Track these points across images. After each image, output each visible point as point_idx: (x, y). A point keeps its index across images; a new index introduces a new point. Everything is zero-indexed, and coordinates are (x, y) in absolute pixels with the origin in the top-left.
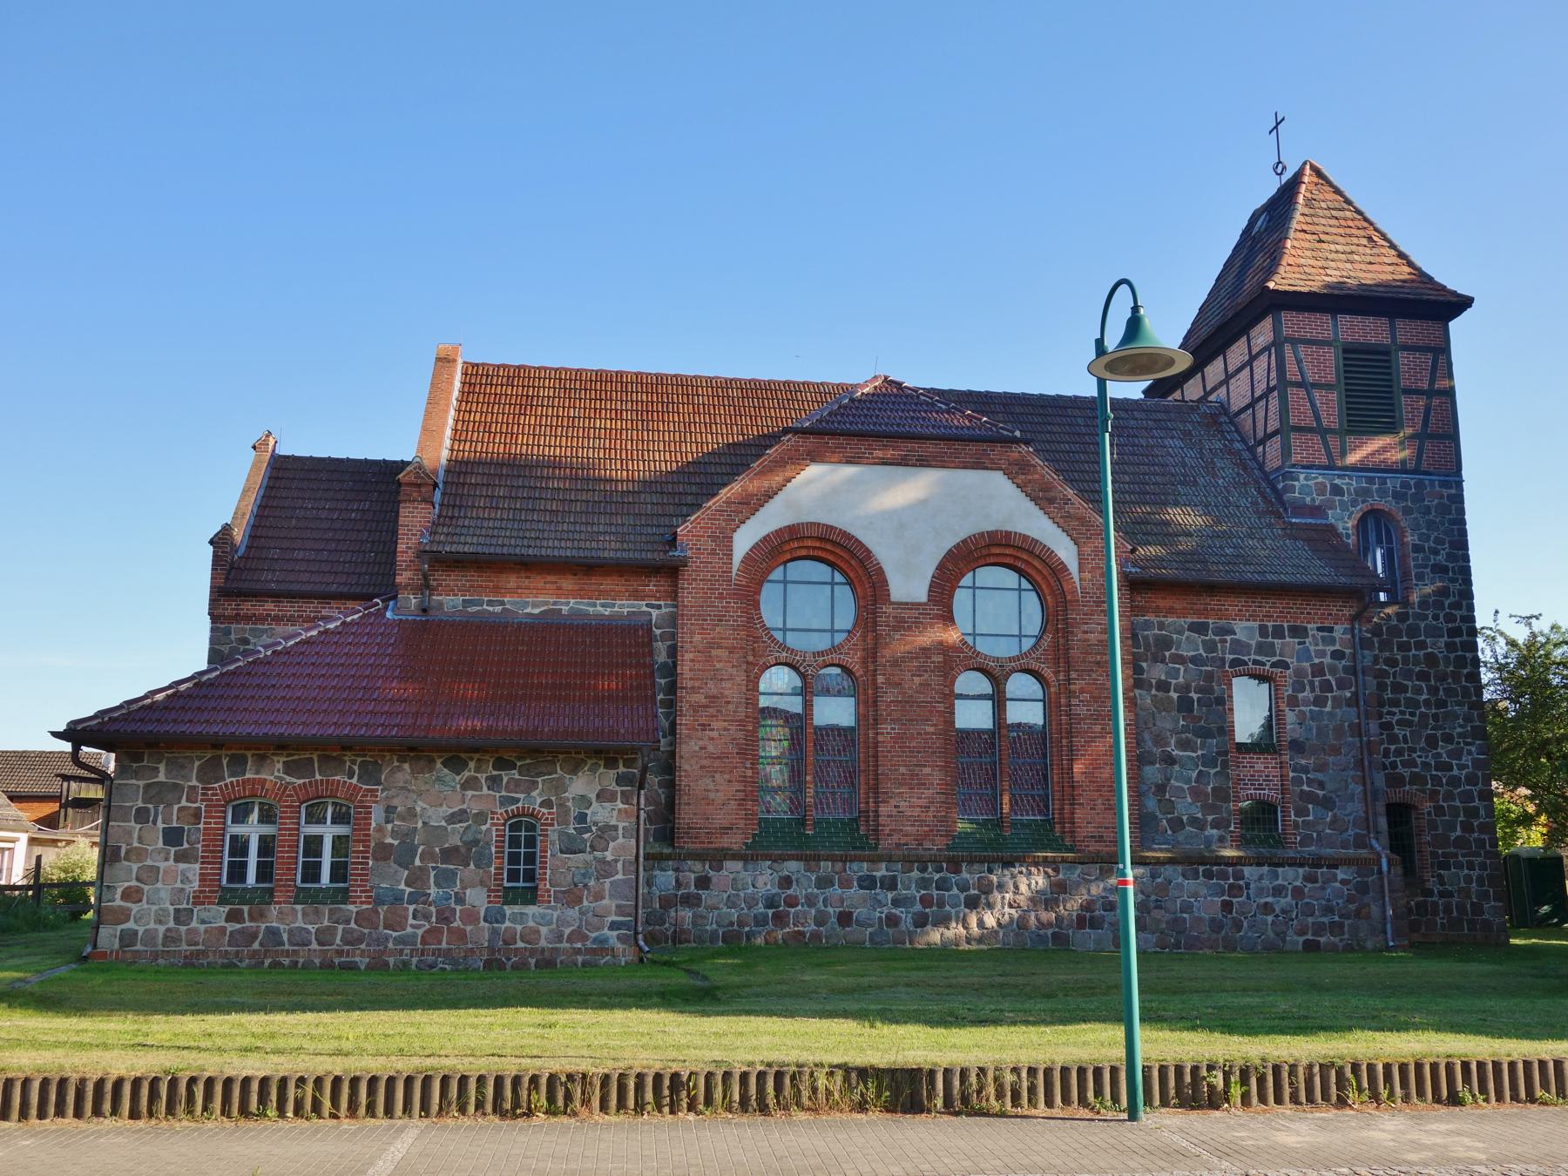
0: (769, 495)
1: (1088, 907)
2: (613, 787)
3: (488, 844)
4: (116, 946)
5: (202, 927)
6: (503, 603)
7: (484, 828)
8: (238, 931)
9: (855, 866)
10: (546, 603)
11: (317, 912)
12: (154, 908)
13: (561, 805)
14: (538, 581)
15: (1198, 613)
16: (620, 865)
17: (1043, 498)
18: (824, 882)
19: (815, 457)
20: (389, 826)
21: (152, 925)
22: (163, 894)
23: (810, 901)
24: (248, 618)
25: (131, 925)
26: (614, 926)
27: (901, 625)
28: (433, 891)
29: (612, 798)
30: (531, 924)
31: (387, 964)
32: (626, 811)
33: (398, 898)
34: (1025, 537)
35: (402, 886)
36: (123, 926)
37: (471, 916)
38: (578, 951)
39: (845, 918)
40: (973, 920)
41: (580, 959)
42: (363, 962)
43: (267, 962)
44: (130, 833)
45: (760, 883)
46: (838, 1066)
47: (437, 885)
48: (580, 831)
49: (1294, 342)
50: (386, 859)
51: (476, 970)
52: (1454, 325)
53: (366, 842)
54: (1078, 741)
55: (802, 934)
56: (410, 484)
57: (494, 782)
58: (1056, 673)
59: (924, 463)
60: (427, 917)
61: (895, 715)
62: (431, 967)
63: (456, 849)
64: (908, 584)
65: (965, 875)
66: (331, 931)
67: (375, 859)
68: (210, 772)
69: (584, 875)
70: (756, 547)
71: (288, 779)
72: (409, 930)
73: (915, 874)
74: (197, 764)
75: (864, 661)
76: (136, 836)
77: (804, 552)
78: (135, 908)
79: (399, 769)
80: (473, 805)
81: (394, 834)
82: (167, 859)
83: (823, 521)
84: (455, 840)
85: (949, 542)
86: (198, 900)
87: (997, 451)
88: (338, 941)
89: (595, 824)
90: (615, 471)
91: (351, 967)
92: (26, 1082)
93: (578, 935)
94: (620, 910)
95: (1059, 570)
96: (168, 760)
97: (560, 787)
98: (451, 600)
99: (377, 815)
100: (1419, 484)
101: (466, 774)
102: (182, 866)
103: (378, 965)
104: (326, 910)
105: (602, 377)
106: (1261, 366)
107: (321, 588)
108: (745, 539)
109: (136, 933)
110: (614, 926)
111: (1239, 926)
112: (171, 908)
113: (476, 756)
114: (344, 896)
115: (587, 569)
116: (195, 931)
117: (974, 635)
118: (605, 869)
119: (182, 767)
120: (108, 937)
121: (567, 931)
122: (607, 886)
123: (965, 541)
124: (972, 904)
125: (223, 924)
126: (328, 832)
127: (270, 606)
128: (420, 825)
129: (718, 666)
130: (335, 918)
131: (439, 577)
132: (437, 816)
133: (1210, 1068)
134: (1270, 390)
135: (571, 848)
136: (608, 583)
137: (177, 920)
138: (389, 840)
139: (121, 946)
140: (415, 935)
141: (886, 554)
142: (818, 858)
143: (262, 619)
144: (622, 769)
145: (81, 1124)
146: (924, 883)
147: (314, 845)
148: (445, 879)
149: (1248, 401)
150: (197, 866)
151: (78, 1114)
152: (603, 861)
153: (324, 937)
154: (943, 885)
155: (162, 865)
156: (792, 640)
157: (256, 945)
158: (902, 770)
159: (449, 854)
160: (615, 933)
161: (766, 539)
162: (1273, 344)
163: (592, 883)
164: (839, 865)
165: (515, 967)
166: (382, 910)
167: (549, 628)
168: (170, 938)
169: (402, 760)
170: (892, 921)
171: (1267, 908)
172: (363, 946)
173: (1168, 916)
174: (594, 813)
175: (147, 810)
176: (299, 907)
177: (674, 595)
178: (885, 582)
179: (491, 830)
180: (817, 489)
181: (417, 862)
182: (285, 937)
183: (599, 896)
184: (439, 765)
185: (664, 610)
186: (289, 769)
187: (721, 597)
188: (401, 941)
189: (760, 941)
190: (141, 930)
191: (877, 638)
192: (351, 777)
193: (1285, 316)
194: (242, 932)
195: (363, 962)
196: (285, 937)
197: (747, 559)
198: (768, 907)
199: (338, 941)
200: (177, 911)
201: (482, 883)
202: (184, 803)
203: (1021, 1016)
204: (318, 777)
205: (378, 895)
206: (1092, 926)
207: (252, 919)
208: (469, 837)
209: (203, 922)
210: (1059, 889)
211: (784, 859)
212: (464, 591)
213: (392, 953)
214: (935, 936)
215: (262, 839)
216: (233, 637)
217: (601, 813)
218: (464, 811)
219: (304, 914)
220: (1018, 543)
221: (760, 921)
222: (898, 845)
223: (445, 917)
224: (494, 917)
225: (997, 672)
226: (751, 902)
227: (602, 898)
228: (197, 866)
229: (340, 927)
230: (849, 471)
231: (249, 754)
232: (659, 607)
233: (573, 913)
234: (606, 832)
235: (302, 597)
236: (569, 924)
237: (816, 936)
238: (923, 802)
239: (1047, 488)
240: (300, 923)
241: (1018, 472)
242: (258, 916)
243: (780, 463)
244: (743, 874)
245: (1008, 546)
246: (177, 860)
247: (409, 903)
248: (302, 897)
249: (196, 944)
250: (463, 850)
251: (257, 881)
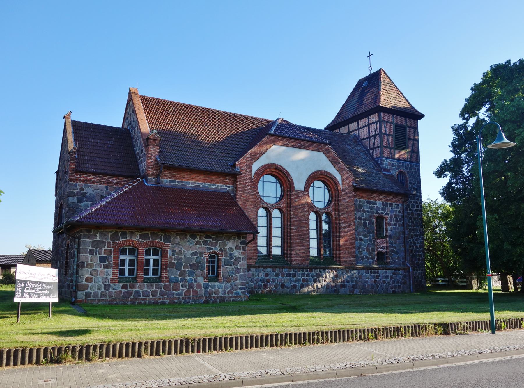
0: (262, 154)
1: (343, 282)
2: (240, 245)
3: (204, 263)
4: (84, 298)
5: (114, 291)
6: (182, 182)
7: (202, 257)
8: (126, 292)
9: (285, 270)
10: (195, 183)
11: (151, 285)
12: (97, 284)
13: (225, 251)
14: (193, 176)
15: (369, 198)
16: (242, 270)
17: (333, 162)
18: (277, 275)
19: (274, 142)
20: (173, 257)
21: (96, 291)
22: (100, 280)
23: (273, 281)
24: (83, 181)
25: (89, 290)
26: (240, 289)
27: (297, 197)
28: (187, 278)
29: (240, 249)
30: (217, 288)
31: (175, 302)
32: (243, 253)
33: (177, 280)
34: (329, 173)
35: (178, 277)
36: (86, 291)
37: (199, 286)
38: (231, 297)
39: (283, 286)
40: (315, 285)
41: (232, 299)
42: (167, 301)
43: (137, 302)
44: (88, 258)
45: (260, 275)
46: (440, 325)
47: (189, 276)
48: (231, 259)
49: (385, 122)
50: (173, 267)
51: (202, 303)
53: (166, 262)
54: (342, 234)
55: (271, 291)
56: (152, 139)
57: (205, 243)
58: (335, 214)
59: (304, 148)
60: (186, 287)
61: (296, 224)
62: (188, 303)
63: (194, 264)
64: (299, 185)
65: (313, 273)
66: (156, 291)
67: (169, 268)
68: (115, 237)
69: (232, 273)
70: (258, 170)
71: (141, 240)
72: (181, 291)
73: (301, 272)
74: (110, 234)
75: (287, 208)
76: (90, 259)
77: (270, 173)
78: (90, 284)
79: (176, 238)
80: (199, 250)
81: (175, 259)
82: (101, 267)
83: (277, 163)
84: (194, 262)
85: (310, 173)
86: (112, 281)
87: (322, 146)
88: (158, 295)
89: (235, 256)
90: (202, 139)
91: (164, 303)
92: (241, 337)
93: (230, 292)
94: (242, 284)
95: (336, 183)
96: (100, 232)
97: (224, 245)
98: (165, 181)
99: (170, 253)
100: (411, 165)
101: (197, 240)
102: (106, 270)
103: (172, 303)
104: (154, 284)
105: (190, 107)
106: (373, 127)
107: (109, 172)
108: (255, 167)
109: (91, 293)
110: (240, 289)
111: (378, 287)
112: (103, 284)
113: (200, 234)
114: (160, 279)
115: (208, 173)
116: (112, 292)
117: (313, 201)
118: (238, 271)
119: (105, 235)
120: (81, 295)
121: (227, 291)
122: (238, 276)
123: (314, 173)
124: (315, 281)
125: (121, 290)
126: (151, 258)
127: (92, 177)
128: (183, 256)
129: (248, 207)
130: (157, 287)
131: (165, 173)
132: (188, 253)
133: (498, 321)
134: (376, 134)
135: (228, 264)
136: (214, 178)
137: (105, 289)
138: (173, 261)
139: (86, 298)
140: (182, 293)
141: (294, 175)
142: (276, 267)
143: (89, 182)
144: (242, 240)
145: (258, 349)
146: (303, 275)
147: (148, 261)
148: (191, 274)
149: (367, 136)
150: (111, 270)
151: (257, 347)
152: (237, 268)
153: (154, 294)
154: (308, 276)
155: (99, 269)
156: (265, 199)
157: (132, 297)
158: (298, 241)
159: (192, 266)
160: (241, 291)
161: (261, 167)
162: (378, 121)
163: (234, 275)
164: (281, 270)
165: (213, 302)
166: (172, 284)
167: (196, 192)
168: (102, 295)
169: (177, 235)
170: (295, 286)
171: (384, 282)
172: (166, 296)
173: (362, 284)
174: (234, 253)
175: (94, 250)
176: (145, 284)
177: (235, 183)
178: (293, 183)
179: (205, 258)
180: (276, 153)
181: (182, 269)
182: (141, 294)
183: (236, 280)
184: (188, 237)
185: (231, 188)
186: (141, 237)
187: (249, 185)
188: (178, 294)
189: (260, 292)
190: (93, 292)
191: (291, 200)
192: (161, 240)
193: (382, 114)
194: (127, 292)
195: (167, 301)
196: (141, 294)
197: (256, 173)
198: (262, 282)
199: (158, 295)
200: (105, 285)
201: (202, 275)
202: (106, 248)
203: (426, 310)
204: (151, 240)
205: (170, 279)
206: (344, 288)
207: (130, 288)
208: (198, 261)
209: (114, 289)
210: (337, 277)
211: (267, 267)
212: (170, 177)
213: (176, 298)
214: (305, 290)
215: (130, 260)
216: (78, 187)
217: (237, 253)
218: (196, 252)
219: (147, 286)
220: (327, 174)
221: (260, 287)
222: (297, 264)
223: (191, 286)
224: (206, 286)
225: (320, 213)
226: (257, 281)
227: (237, 280)
228: (111, 270)
229: (159, 290)
230: (284, 148)
231: (128, 231)
232: (229, 187)
233: (229, 285)
234: (238, 259)
235: (103, 175)
236: (228, 288)
237: (275, 291)
238: (303, 251)
239: (334, 159)
240: (146, 289)
241: (327, 153)
242: (132, 287)
243: (265, 144)
244: (255, 272)
245: (325, 175)
246: (104, 268)
247: (180, 282)
248: (146, 280)
249: (112, 297)
250: (196, 265)
251: (129, 275)
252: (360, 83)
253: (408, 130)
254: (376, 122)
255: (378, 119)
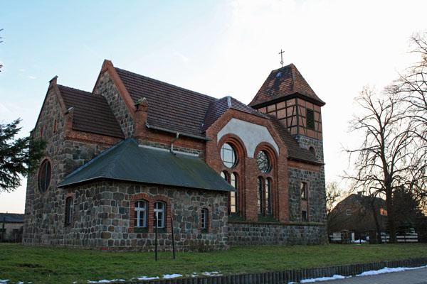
17: (273, 136)
24: (78, 140)
25: (111, 239)
28: (186, 229)
37: (194, 237)
49: (300, 106)
52: (322, 107)
57: (198, 199)
66: (163, 241)
68: (131, 191)
84: (190, 215)
86: (129, 231)
97: (213, 201)
99: (173, 206)
101: (192, 196)
102: (125, 220)
106: (290, 110)
108: (220, 136)
121: (215, 241)
125: (135, 238)
134: (293, 116)
141: (246, 145)
148: (189, 226)
149: (285, 116)
155: (119, 219)
157: (145, 245)
161: (224, 136)
168: (123, 243)
171: (307, 235)
177: (204, 149)
179: (199, 211)
193: (298, 99)
207: (144, 237)
241: (269, 128)
252: (273, 75)
253: (315, 114)
254: (293, 106)
255: (295, 103)
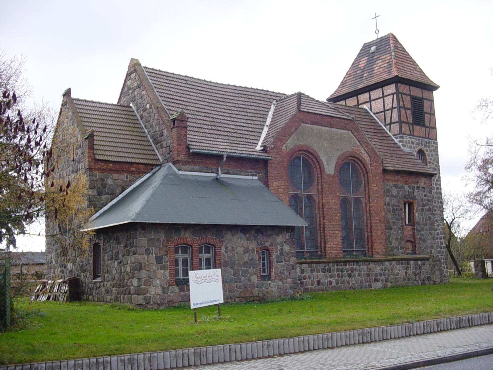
15: (396, 181)
18: (312, 271)
37: (253, 286)
39: (319, 283)
49: (402, 94)
52: (434, 92)
65: (347, 267)
73: (336, 267)
100: (429, 142)
106: (388, 100)
111: (409, 280)
129: (281, 195)
134: (393, 108)
146: (338, 270)
162: (395, 93)
193: (399, 85)
201: (255, 274)
208: (250, 258)
238: (336, 243)
252: (366, 47)
253: (426, 103)
254: (393, 94)
255: (394, 91)
